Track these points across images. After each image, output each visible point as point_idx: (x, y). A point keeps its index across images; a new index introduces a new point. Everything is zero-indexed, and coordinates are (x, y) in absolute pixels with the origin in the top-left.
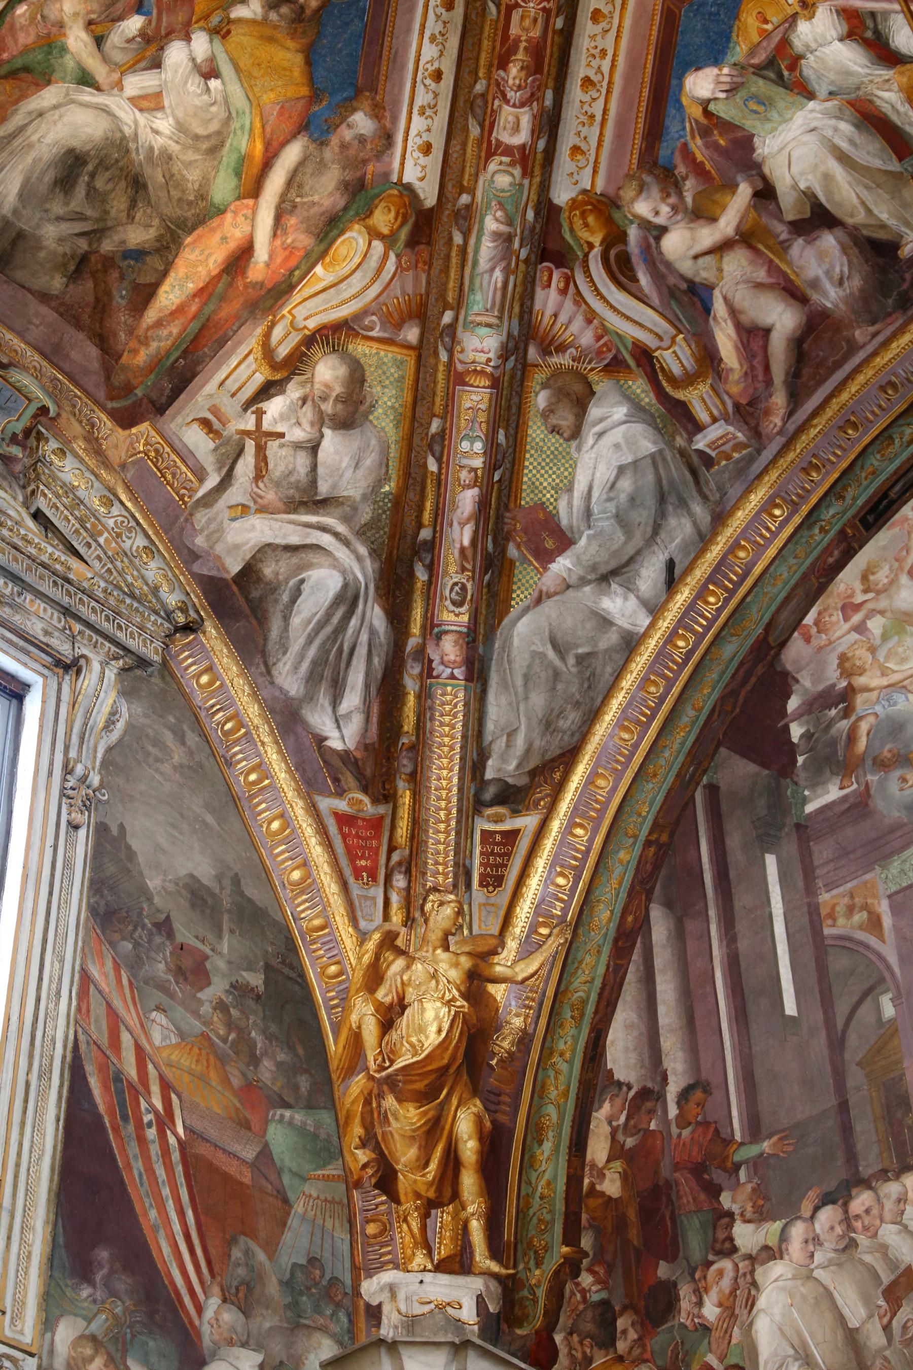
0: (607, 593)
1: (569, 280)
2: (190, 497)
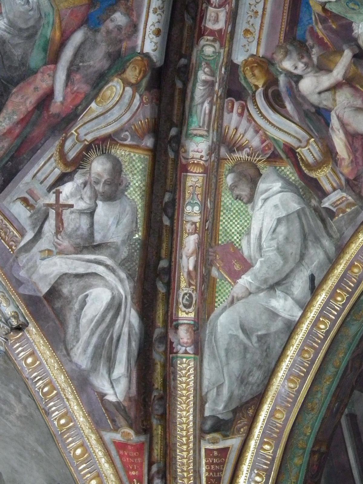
0: (274, 297)
1: (244, 108)
2: (16, 246)
